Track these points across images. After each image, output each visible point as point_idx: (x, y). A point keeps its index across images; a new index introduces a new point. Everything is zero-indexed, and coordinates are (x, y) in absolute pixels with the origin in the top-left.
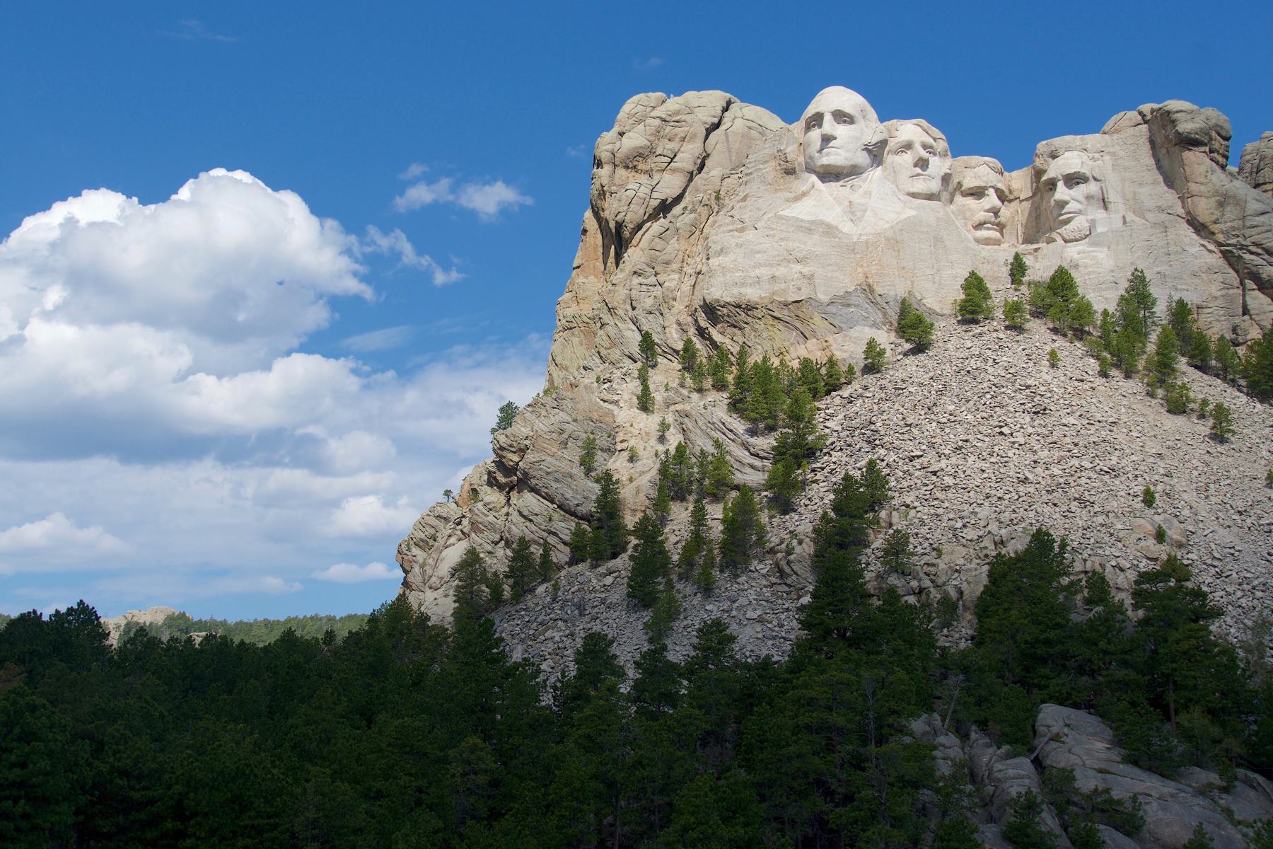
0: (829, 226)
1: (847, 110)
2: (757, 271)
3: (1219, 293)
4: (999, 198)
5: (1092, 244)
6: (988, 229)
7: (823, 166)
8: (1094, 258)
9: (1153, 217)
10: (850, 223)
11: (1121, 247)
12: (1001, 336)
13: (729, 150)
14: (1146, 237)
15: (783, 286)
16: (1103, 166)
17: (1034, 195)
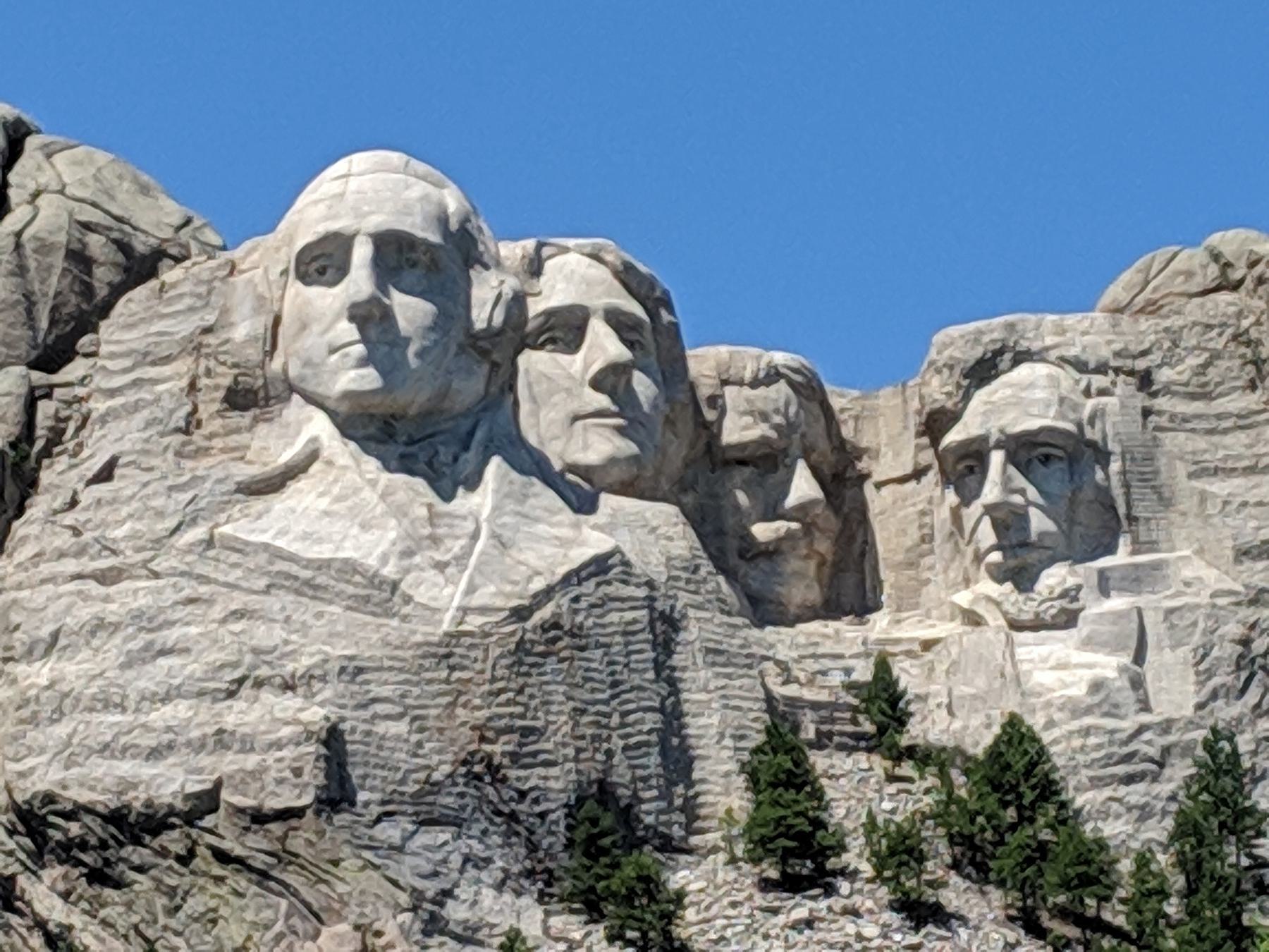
0: (374, 581)
1: (420, 234)
2: (168, 710)
4: (816, 471)
5: (1088, 643)
7: (347, 395)
8: (1097, 686)
9: (1259, 573)
10: (431, 574)
11: (1168, 655)
12: (870, 930)
13: (28, 296)
14: (1233, 629)
15: (251, 761)
16: (1115, 412)
17: (918, 474)
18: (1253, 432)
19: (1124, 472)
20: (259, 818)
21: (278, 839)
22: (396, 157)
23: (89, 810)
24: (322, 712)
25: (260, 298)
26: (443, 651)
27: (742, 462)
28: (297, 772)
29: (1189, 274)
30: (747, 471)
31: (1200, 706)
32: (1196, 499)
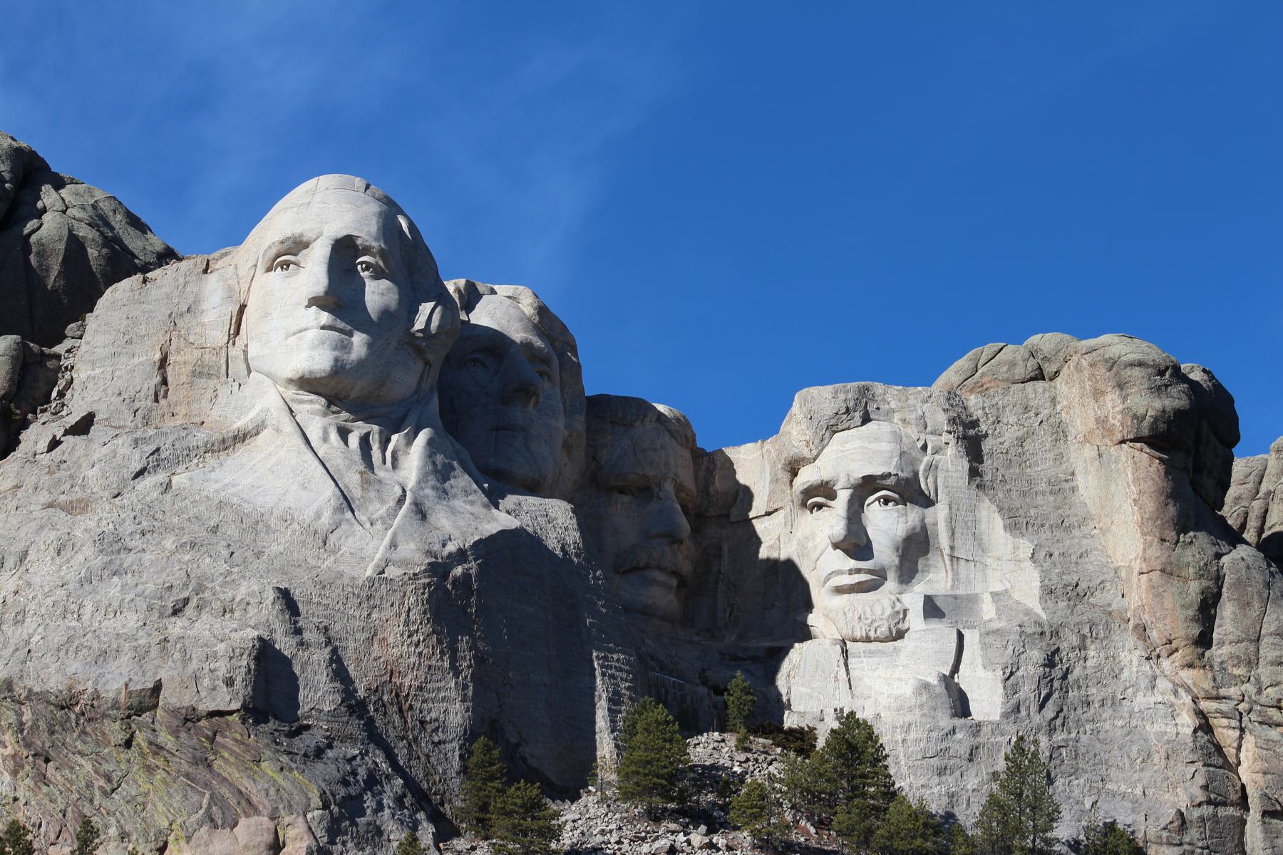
3: (1196, 813)
6: (653, 582)
11: (981, 673)
14: (1036, 655)
18: (1060, 498)
19: (950, 519)
20: (189, 718)
21: (207, 737)
22: (359, 182)
23: (42, 697)
24: (256, 633)
25: (230, 289)
26: (364, 594)
27: (622, 492)
28: (230, 682)
29: (1013, 364)
30: (626, 499)
31: (1005, 715)
32: (1010, 546)
